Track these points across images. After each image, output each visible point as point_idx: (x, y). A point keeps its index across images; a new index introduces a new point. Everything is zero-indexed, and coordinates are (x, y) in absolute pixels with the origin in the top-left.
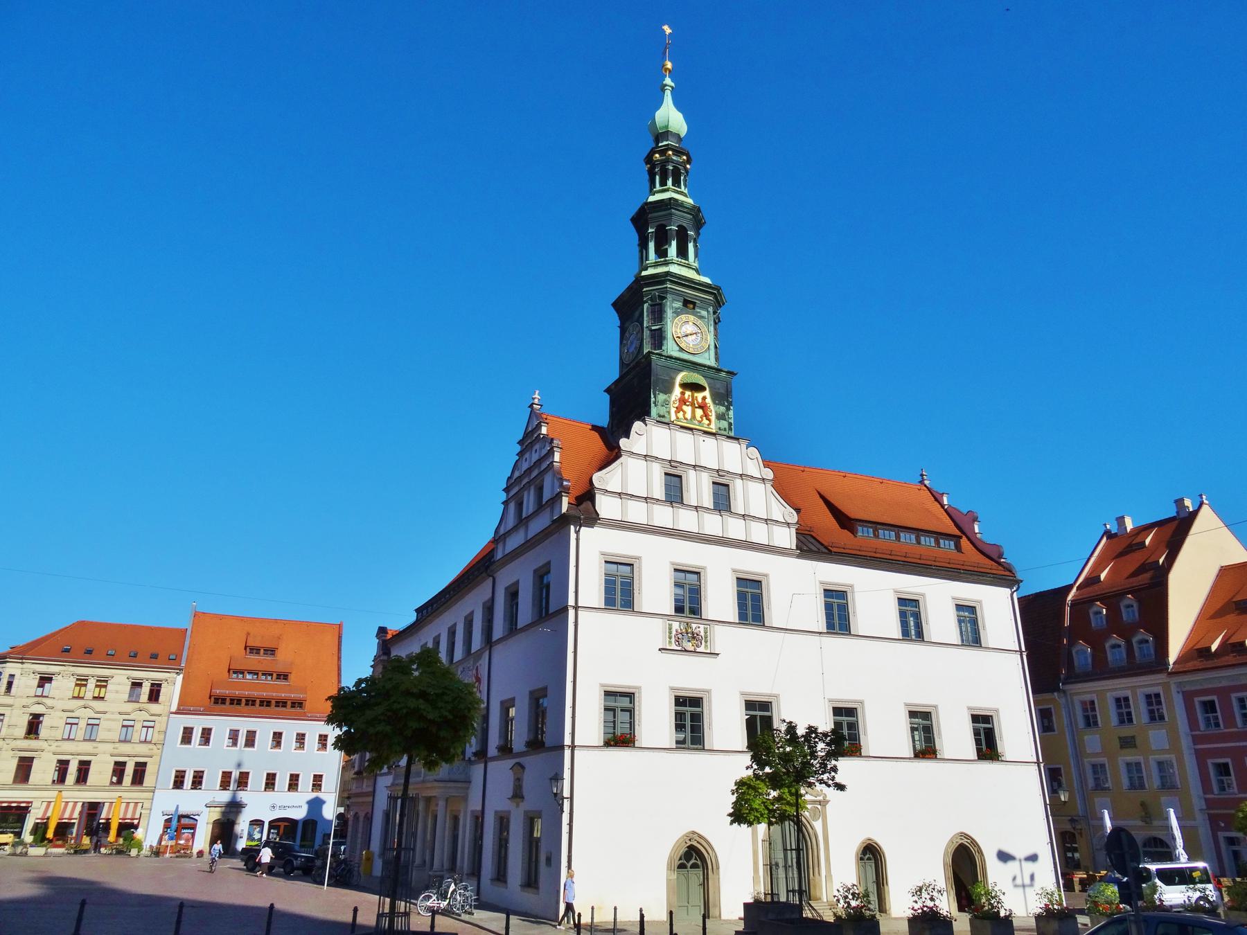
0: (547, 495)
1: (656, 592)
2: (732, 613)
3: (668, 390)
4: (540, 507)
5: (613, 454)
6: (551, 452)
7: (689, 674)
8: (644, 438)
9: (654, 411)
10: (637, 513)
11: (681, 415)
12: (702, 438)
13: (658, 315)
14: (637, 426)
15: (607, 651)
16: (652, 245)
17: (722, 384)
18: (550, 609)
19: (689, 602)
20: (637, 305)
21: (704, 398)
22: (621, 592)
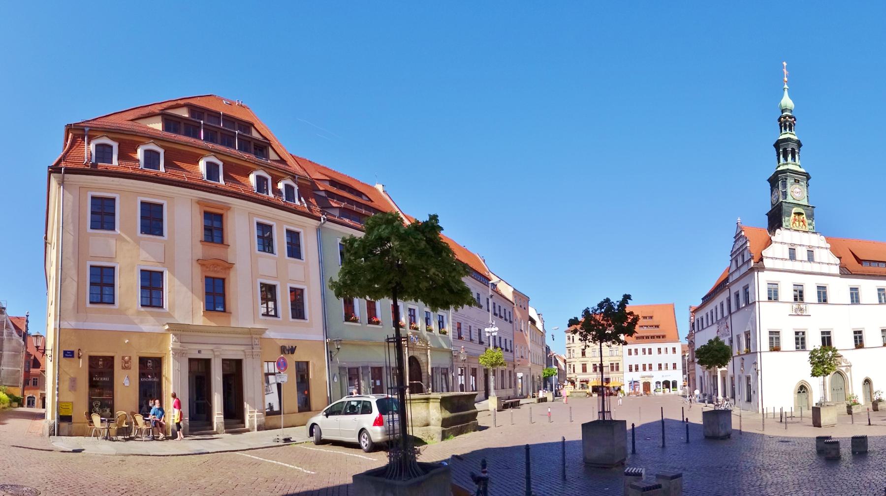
0: (746, 260)
1: (786, 293)
2: (815, 299)
3: (789, 216)
4: (744, 263)
5: (769, 242)
6: (746, 243)
7: (800, 324)
8: (781, 235)
9: (784, 224)
10: (779, 265)
13: (785, 186)
14: (778, 231)
15: (771, 316)
16: (781, 156)
17: (810, 212)
18: (747, 301)
19: (799, 296)
20: (776, 181)
22: (773, 295)
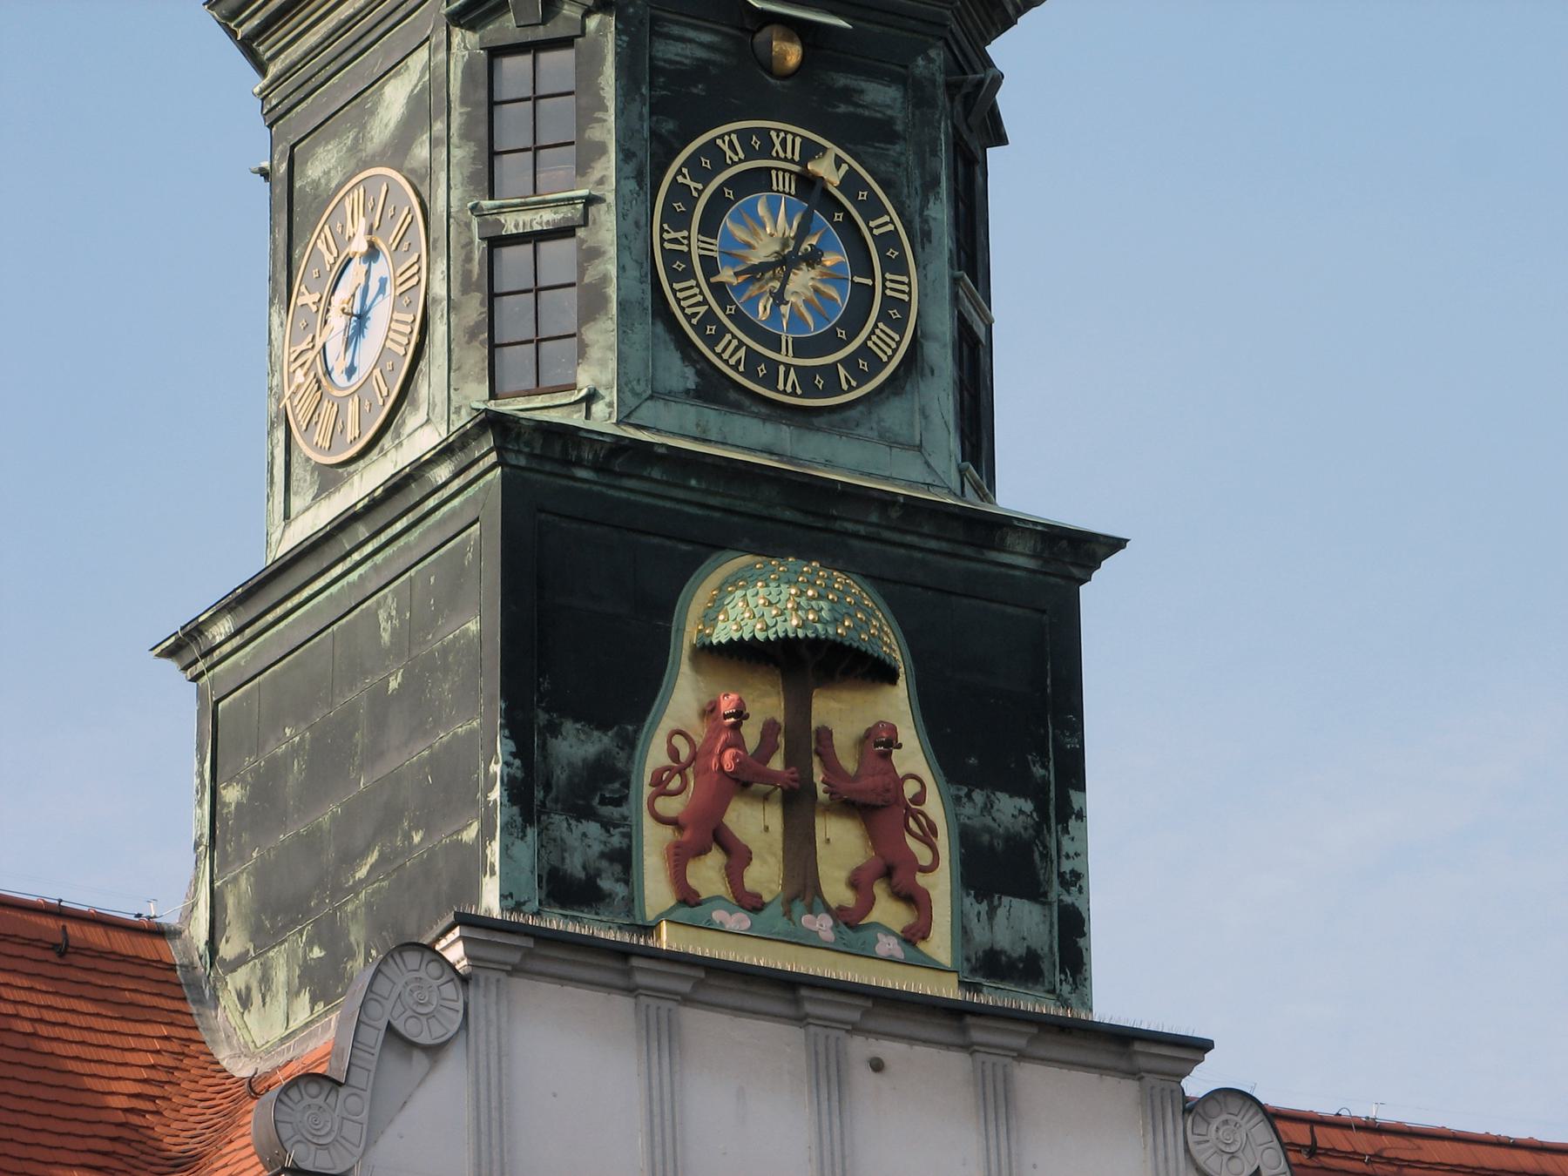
3: (629, 696)
11: (707, 874)
12: (861, 1048)
21: (881, 742)
